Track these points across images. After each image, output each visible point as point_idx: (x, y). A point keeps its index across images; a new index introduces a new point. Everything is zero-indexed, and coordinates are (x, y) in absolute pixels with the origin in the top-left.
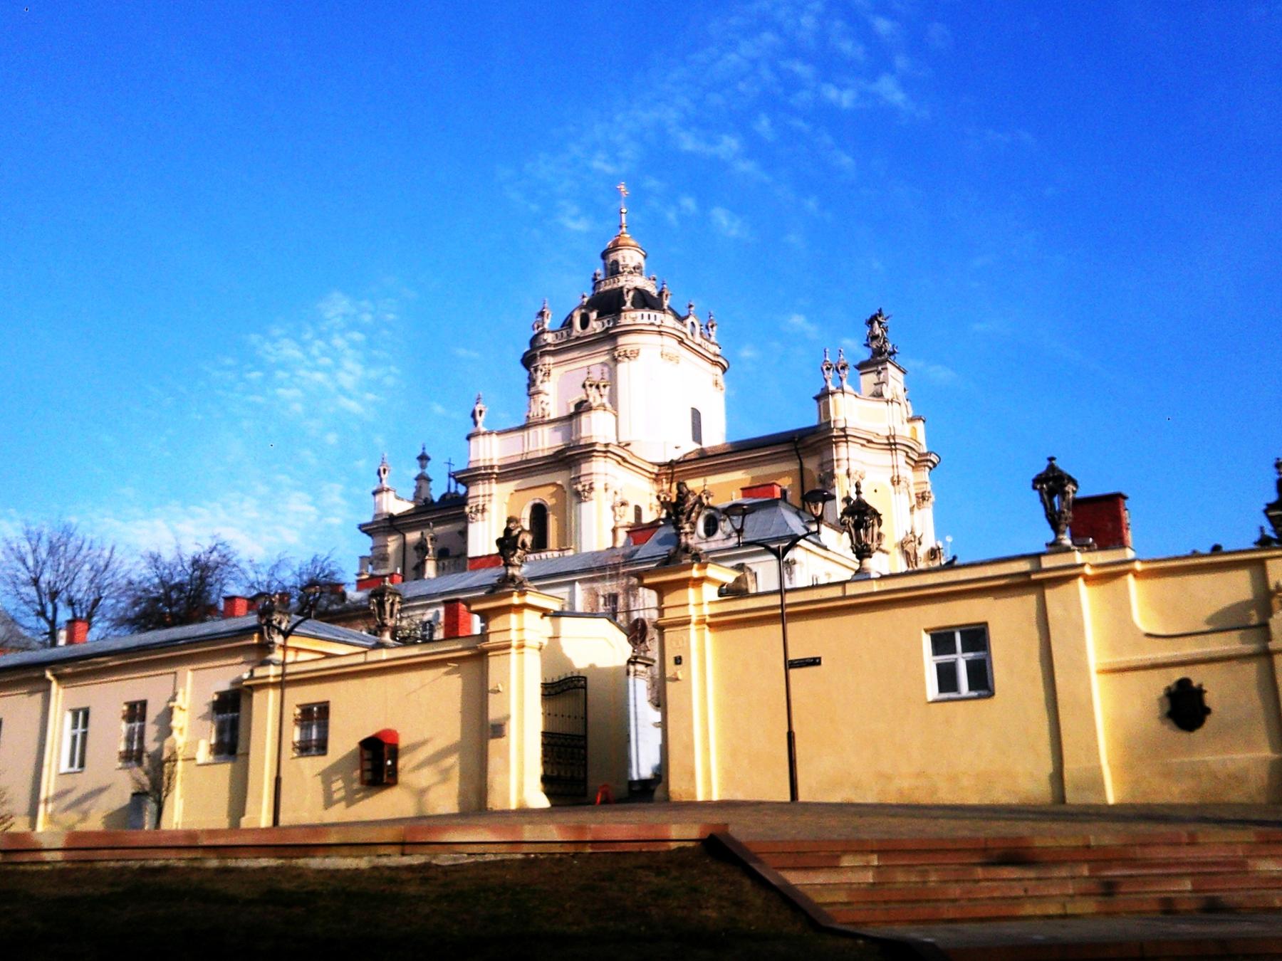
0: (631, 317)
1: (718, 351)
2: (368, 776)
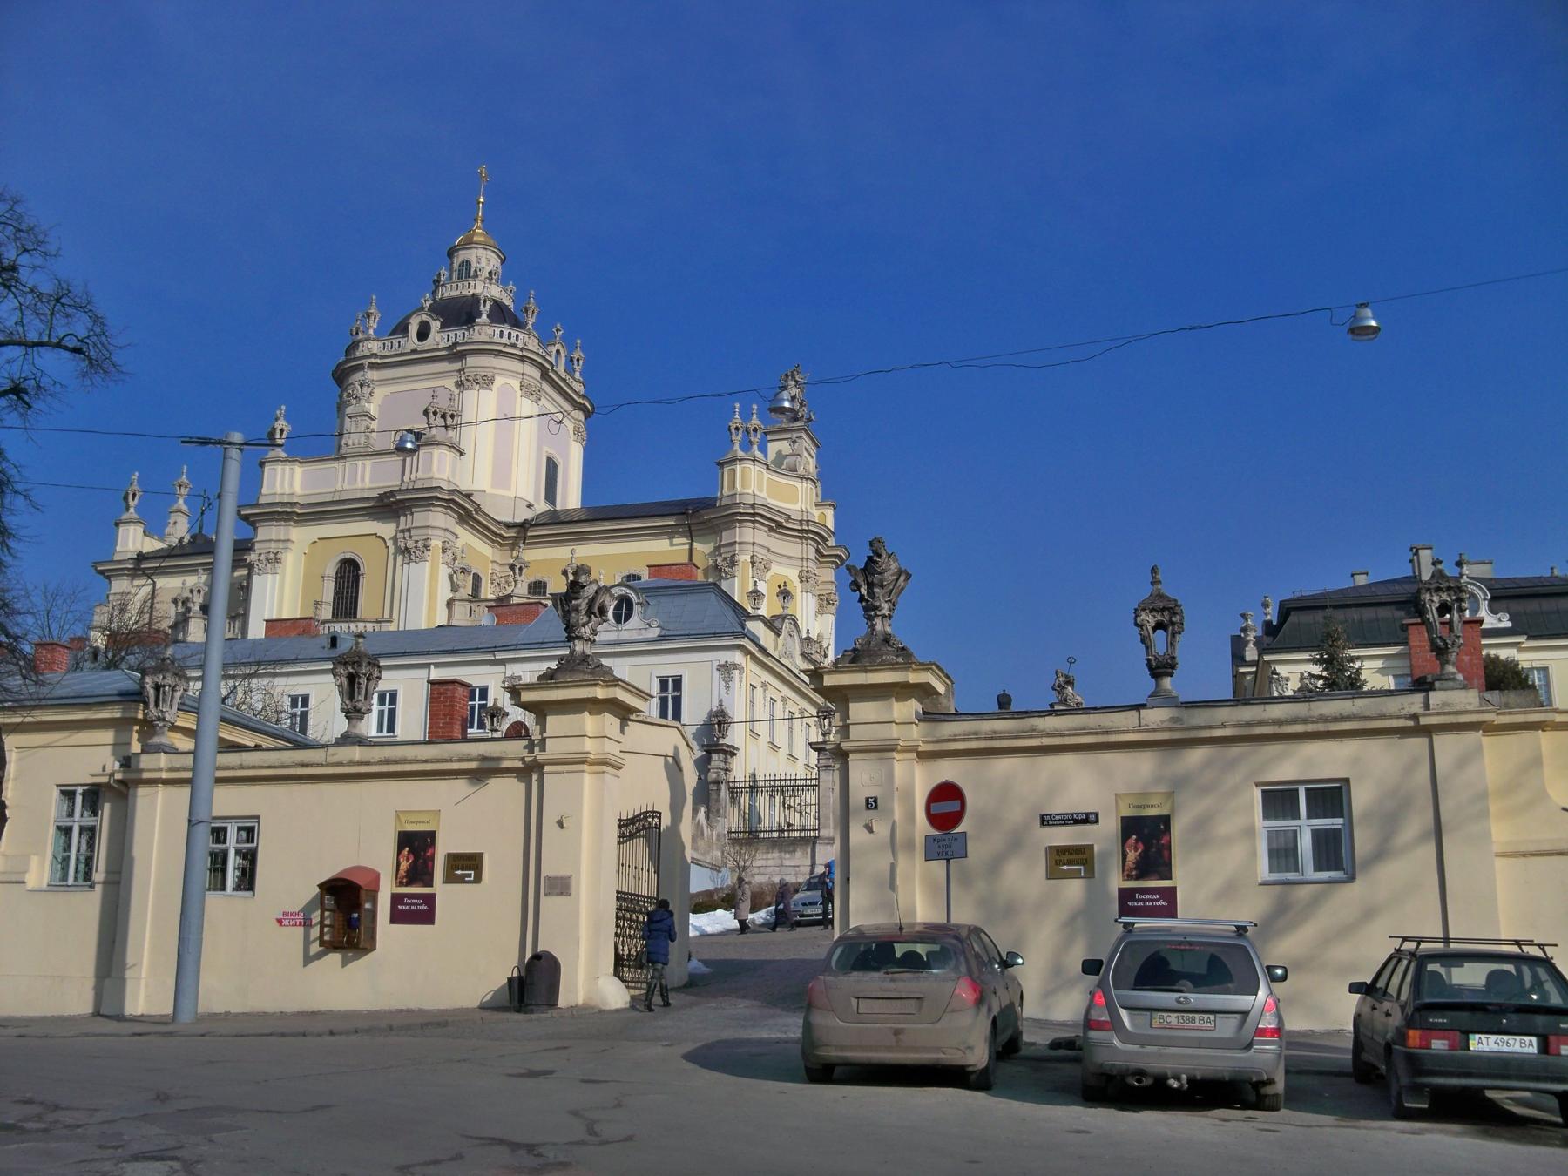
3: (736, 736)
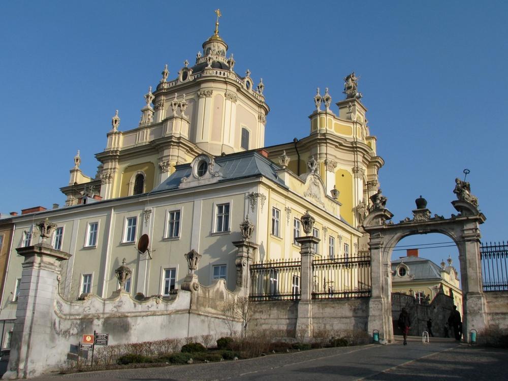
1: (263, 100)
3: (261, 235)
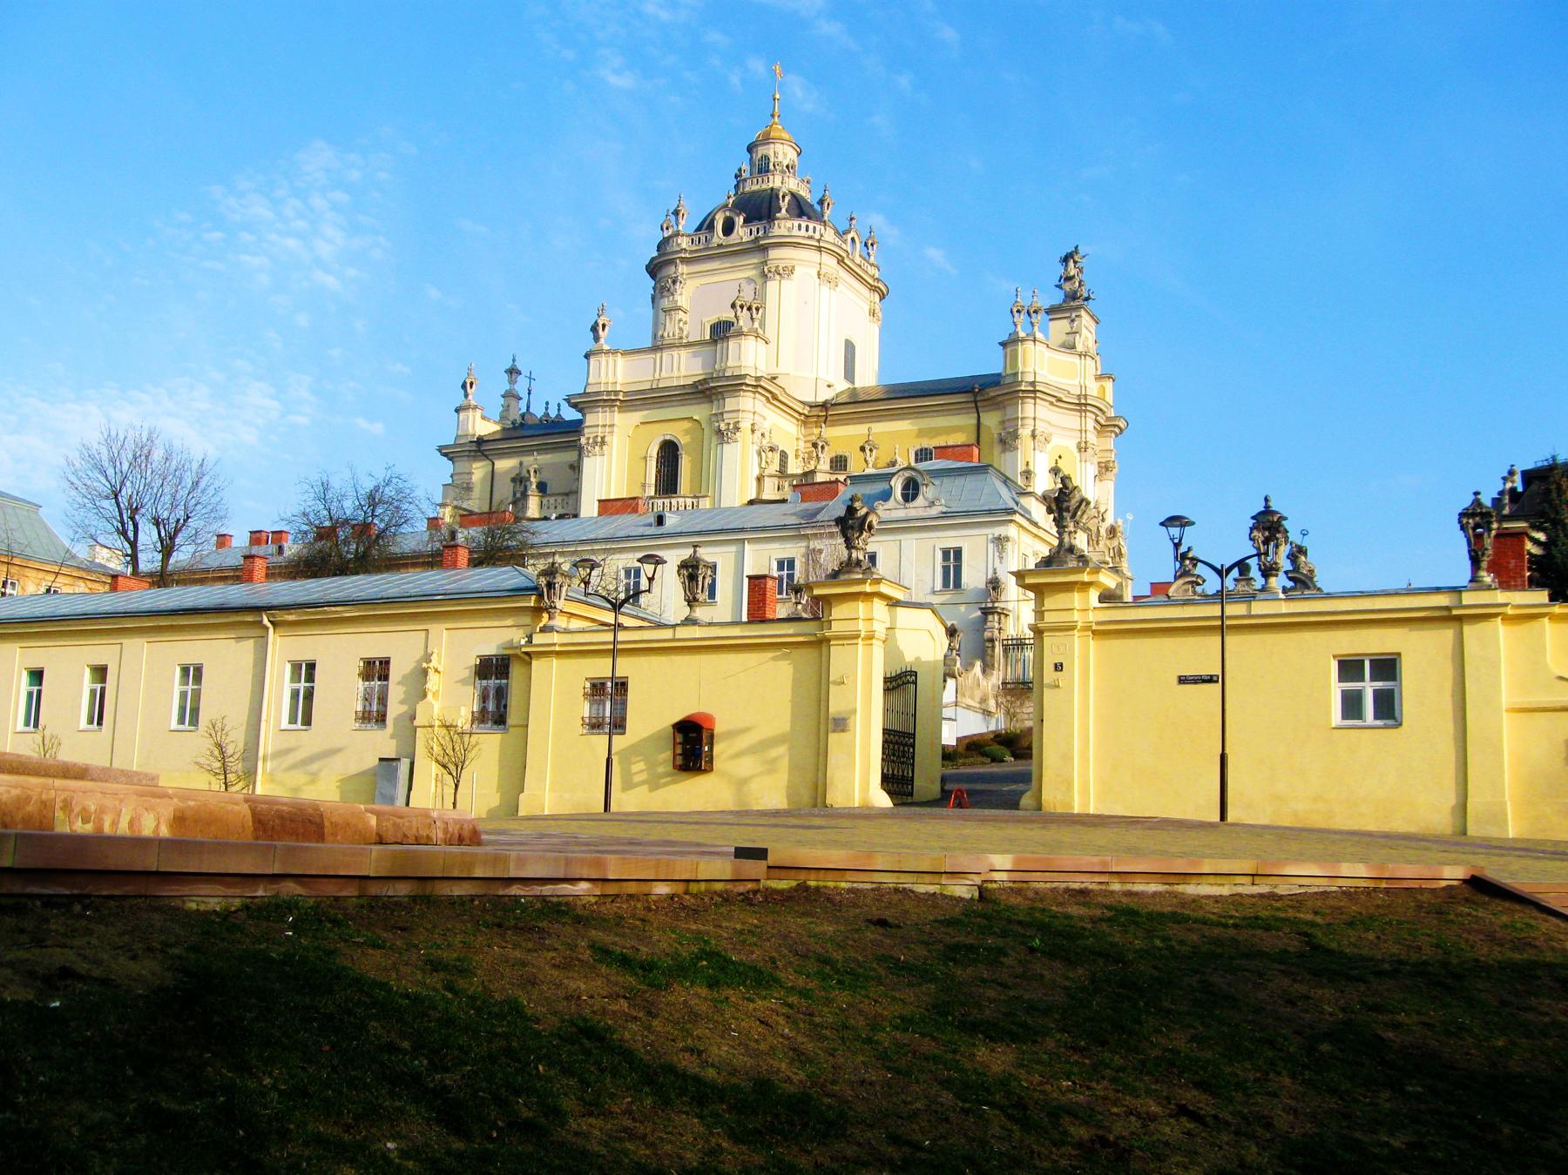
0: (785, 226)
2: (679, 761)
